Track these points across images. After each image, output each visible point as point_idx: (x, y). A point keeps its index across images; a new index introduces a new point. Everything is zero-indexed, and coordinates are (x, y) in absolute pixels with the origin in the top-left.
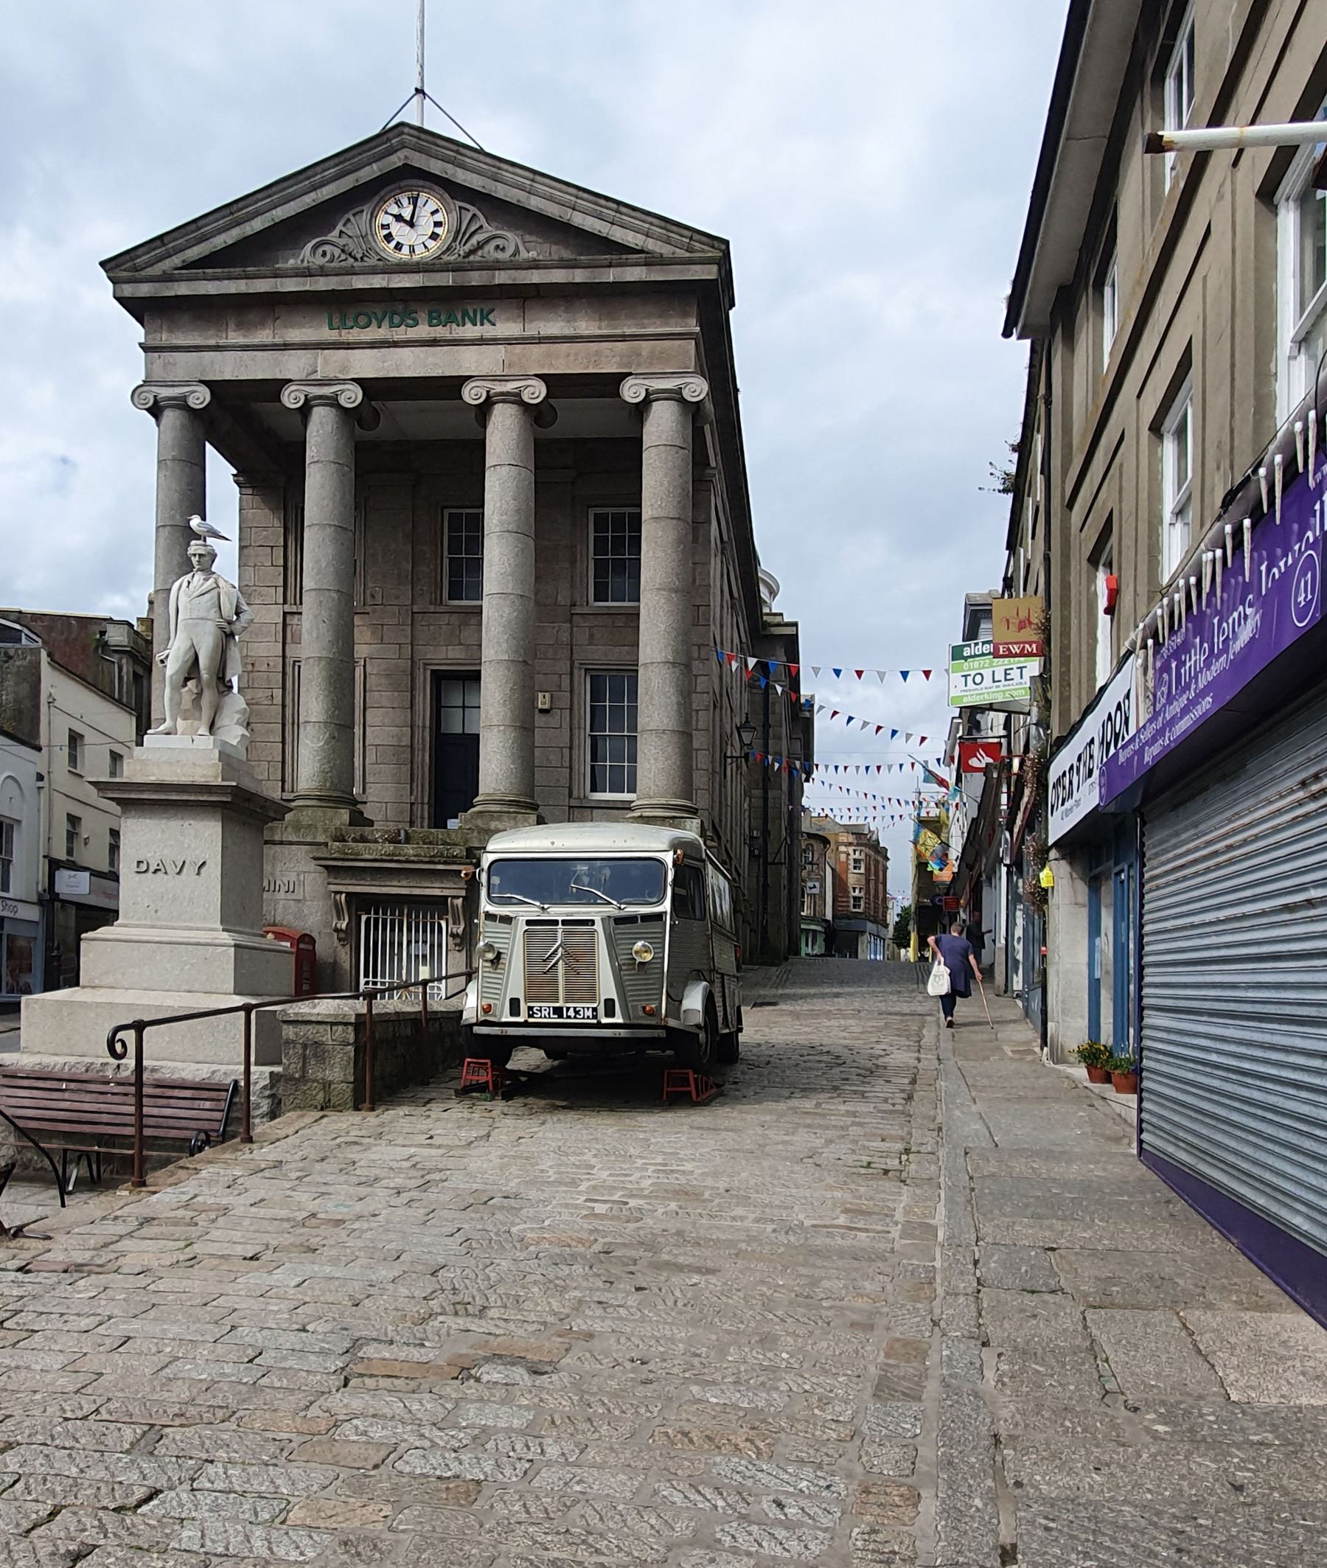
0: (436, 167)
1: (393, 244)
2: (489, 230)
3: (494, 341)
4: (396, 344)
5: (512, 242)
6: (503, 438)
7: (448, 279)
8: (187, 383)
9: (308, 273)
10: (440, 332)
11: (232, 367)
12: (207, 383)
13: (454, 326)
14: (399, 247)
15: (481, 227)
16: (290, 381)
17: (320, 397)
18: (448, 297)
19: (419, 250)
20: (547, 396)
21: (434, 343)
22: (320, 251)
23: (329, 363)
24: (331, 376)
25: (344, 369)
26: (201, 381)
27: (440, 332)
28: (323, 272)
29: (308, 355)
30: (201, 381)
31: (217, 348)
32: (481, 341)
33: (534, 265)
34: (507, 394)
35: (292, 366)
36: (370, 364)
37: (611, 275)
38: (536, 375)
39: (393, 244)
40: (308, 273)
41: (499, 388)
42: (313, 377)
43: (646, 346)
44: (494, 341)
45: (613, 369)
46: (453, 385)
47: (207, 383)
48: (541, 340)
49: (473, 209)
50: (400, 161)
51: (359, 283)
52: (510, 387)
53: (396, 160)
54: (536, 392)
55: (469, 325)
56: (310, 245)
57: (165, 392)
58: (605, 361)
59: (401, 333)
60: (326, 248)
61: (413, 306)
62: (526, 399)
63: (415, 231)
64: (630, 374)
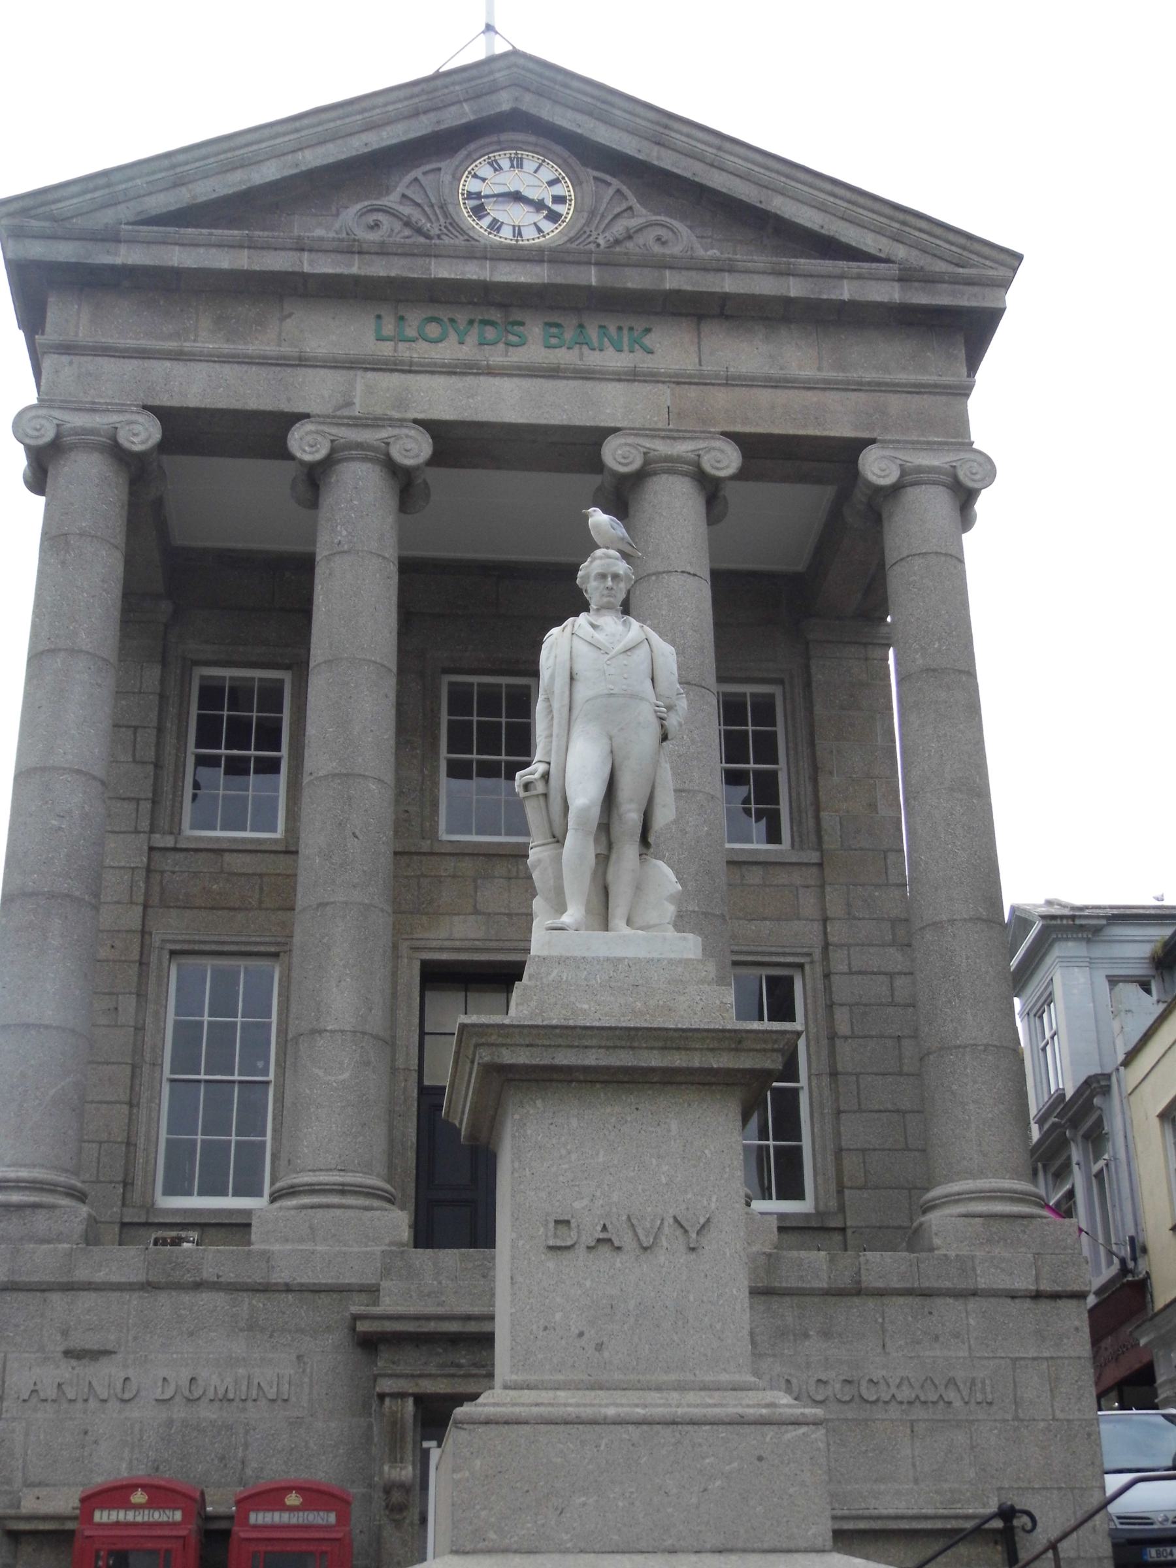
1: (485, 222)
2: (643, 215)
3: (653, 378)
4: (490, 371)
5: (684, 238)
8: (121, 409)
9: (353, 249)
10: (564, 357)
11: (198, 387)
13: (585, 349)
14: (496, 226)
15: (630, 208)
16: (307, 416)
17: (359, 446)
21: (553, 373)
22: (371, 219)
23: (372, 392)
24: (379, 411)
26: (145, 407)
27: (564, 357)
28: (383, 251)
29: (340, 376)
30: (145, 407)
31: (178, 356)
32: (633, 376)
34: (678, 459)
36: (447, 399)
37: (846, 292)
38: (724, 434)
39: (485, 222)
40: (353, 249)
41: (662, 448)
42: (346, 412)
43: (895, 403)
44: (653, 378)
45: (847, 432)
48: (730, 381)
49: (616, 183)
50: (497, 107)
51: (442, 270)
52: (683, 448)
53: (504, 102)
54: (725, 460)
55: (610, 351)
56: (359, 206)
57: (78, 420)
58: (837, 419)
59: (497, 356)
60: (380, 216)
61: (517, 315)
62: (707, 467)
63: (518, 203)
64: (873, 441)
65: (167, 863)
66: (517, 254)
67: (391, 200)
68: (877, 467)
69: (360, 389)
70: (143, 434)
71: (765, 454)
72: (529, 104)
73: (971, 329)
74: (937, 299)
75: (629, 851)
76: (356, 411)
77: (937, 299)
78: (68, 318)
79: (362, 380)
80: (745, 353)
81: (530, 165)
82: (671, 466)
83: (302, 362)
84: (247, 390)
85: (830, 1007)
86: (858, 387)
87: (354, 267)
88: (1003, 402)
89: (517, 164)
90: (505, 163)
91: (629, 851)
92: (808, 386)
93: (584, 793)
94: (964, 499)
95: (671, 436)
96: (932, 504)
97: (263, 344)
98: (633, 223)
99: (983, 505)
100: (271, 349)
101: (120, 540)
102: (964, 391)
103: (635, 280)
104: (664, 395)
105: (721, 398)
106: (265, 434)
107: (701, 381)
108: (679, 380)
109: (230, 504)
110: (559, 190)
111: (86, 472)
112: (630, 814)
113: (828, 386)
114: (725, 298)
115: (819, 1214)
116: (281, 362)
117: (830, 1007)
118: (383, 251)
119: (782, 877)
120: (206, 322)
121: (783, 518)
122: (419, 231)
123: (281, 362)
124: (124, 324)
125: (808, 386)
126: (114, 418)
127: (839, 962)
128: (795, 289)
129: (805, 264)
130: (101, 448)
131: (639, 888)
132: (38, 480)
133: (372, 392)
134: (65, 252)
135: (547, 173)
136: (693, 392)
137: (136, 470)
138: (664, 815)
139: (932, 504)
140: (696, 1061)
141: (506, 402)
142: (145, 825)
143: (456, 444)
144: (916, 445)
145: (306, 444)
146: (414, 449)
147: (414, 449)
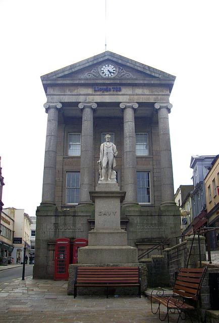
0: (114, 59)
4: (105, 95)
5: (131, 75)
6: (129, 116)
8: (57, 103)
10: (115, 93)
11: (66, 99)
18: (115, 86)
20: (139, 107)
21: (114, 95)
25: (93, 100)
31: (64, 95)
35: (81, 99)
36: (99, 99)
41: (128, 104)
43: (159, 97)
46: (117, 104)
52: (130, 104)
54: (136, 106)
57: (51, 104)
63: (107, 70)
65: (65, 160)
66: (108, 79)
68: (157, 106)
69: (89, 98)
70: (59, 106)
71: (141, 104)
72: (110, 58)
73: (169, 87)
74: (165, 82)
75: (110, 170)
76: (87, 101)
77: (165, 82)
78: (51, 91)
79: (88, 97)
80: (139, 91)
81: (110, 66)
82: (129, 107)
83: (80, 95)
84: (73, 99)
85: (153, 177)
86: (155, 95)
87: (87, 82)
88: (174, 97)
89: (108, 66)
90: (107, 66)
91: (110, 170)
92: (148, 95)
93: (104, 165)
94: (169, 111)
95: (129, 103)
96: (164, 111)
97: (75, 92)
98: (124, 73)
99: (171, 110)
100: (76, 93)
101: (57, 120)
102: (169, 95)
103: (124, 82)
104: (128, 96)
105: (136, 97)
107: (133, 95)
108: (130, 95)
109: (71, 112)
110: (114, 69)
111: (52, 111)
112: (110, 166)
113: (150, 95)
114: (136, 84)
115: (152, 204)
116: (77, 95)
117: (153, 177)
119: (147, 159)
121: (145, 112)
122: (95, 76)
123: (77, 95)
124: (57, 91)
125: (148, 95)
126: (56, 104)
127: (155, 171)
128: (146, 82)
129: (148, 79)
130: (54, 108)
131: (111, 174)
132: (47, 111)
134: (49, 82)
135: (113, 67)
136: (132, 96)
137: (59, 110)
138: (114, 165)
140: (114, 195)
141: (107, 98)
142: (62, 155)
143: (100, 104)
144: (162, 103)
145: (81, 106)
146: (95, 106)
147: (95, 106)
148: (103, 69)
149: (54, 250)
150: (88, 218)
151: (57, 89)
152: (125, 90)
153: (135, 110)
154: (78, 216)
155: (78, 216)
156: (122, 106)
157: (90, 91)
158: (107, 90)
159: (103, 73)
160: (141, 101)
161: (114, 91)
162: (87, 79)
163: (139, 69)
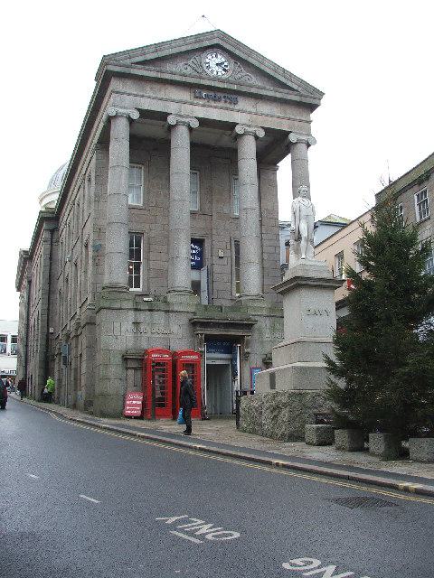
0: (228, 47)
2: (244, 73)
7: (235, 87)
12: (139, 110)
18: (227, 94)
19: (219, 74)
23: (186, 109)
33: (264, 88)
35: (171, 108)
37: (289, 97)
43: (296, 123)
45: (286, 129)
47: (139, 110)
51: (202, 82)
53: (215, 41)
59: (213, 104)
63: (214, 64)
67: (190, 62)
68: (292, 138)
69: (185, 110)
72: (220, 42)
73: (312, 107)
74: (307, 101)
77: (307, 101)
80: (265, 108)
84: (157, 106)
94: (309, 145)
95: (249, 126)
96: (302, 147)
97: (161, 95)
102: (309, 122)
103: (244, 89)
104: (249, 116)
106: (163, 116)
118: (190, 76)
120: (148, 89)
128: (278, 95)
133: (186, 109)
134: (117, 69)
139: (304, 146)
141: (215, 113)
144: (301, 134)
148: (208, 61)
149: (135, 369)
150: (191, 316)
151: (129, 83)
152: (243, 104)
153: (131, 121)
154: (173, 312)
155: (173, 312)
156: (239, 130)
157: (185, 95)
158: (217, 100)
159: (208, 67)
160: (146, 107)
161: (226, 102)
162: (184, 75)
163: (268, 71)
